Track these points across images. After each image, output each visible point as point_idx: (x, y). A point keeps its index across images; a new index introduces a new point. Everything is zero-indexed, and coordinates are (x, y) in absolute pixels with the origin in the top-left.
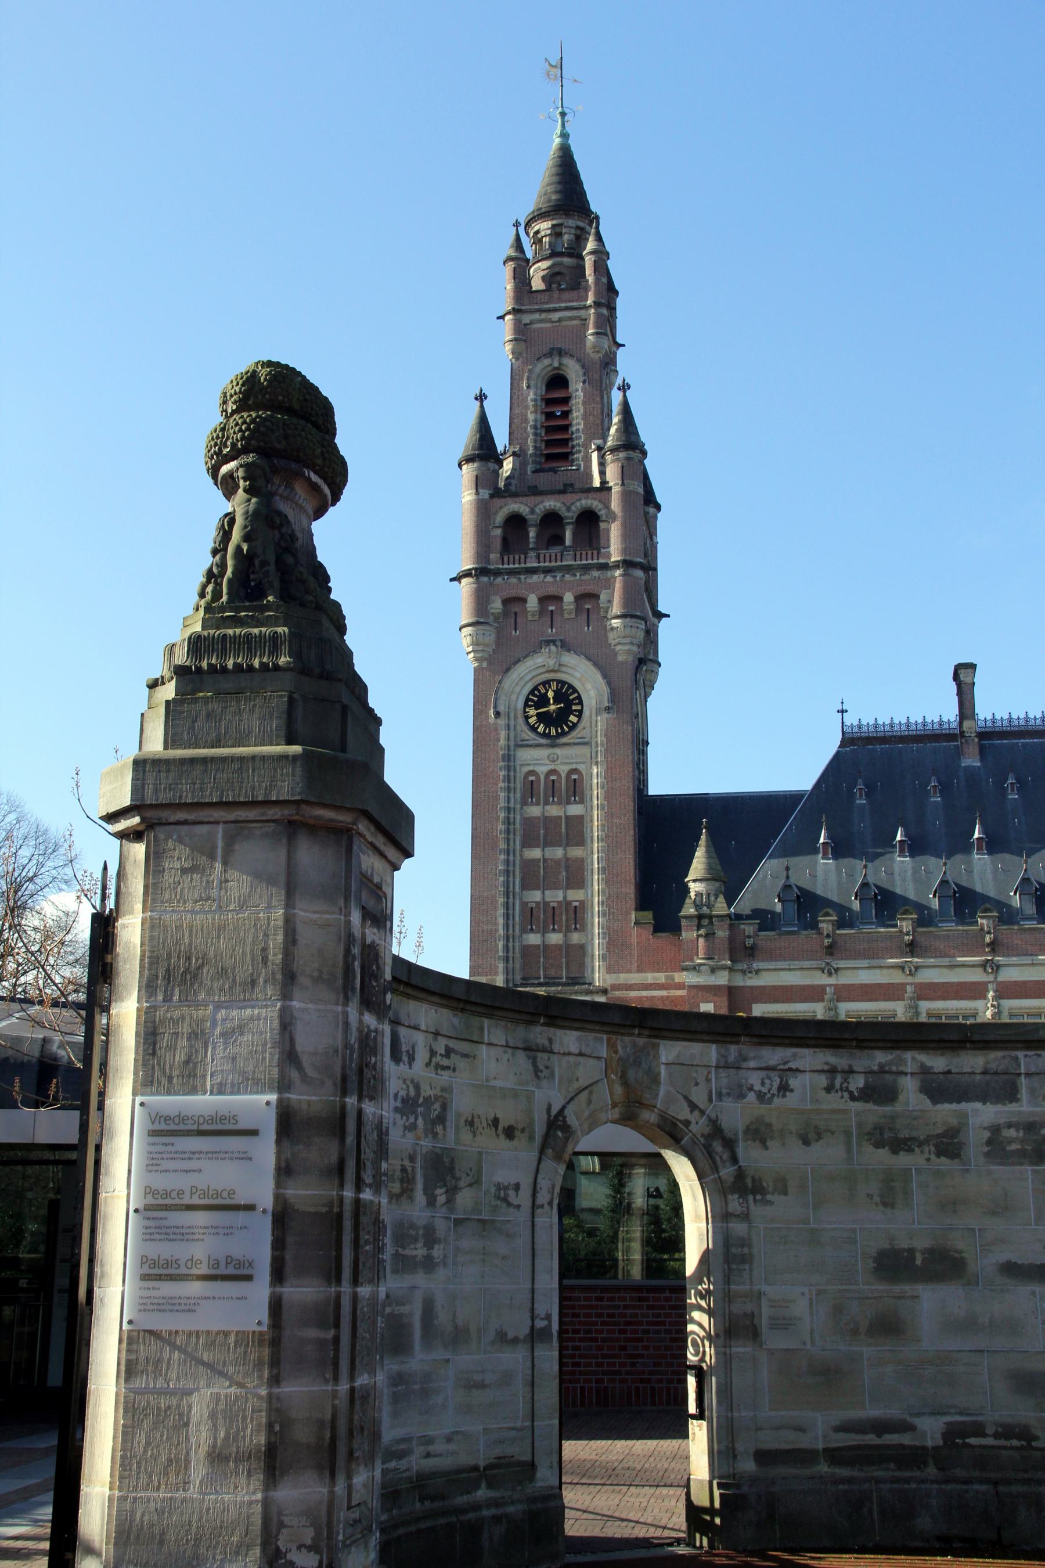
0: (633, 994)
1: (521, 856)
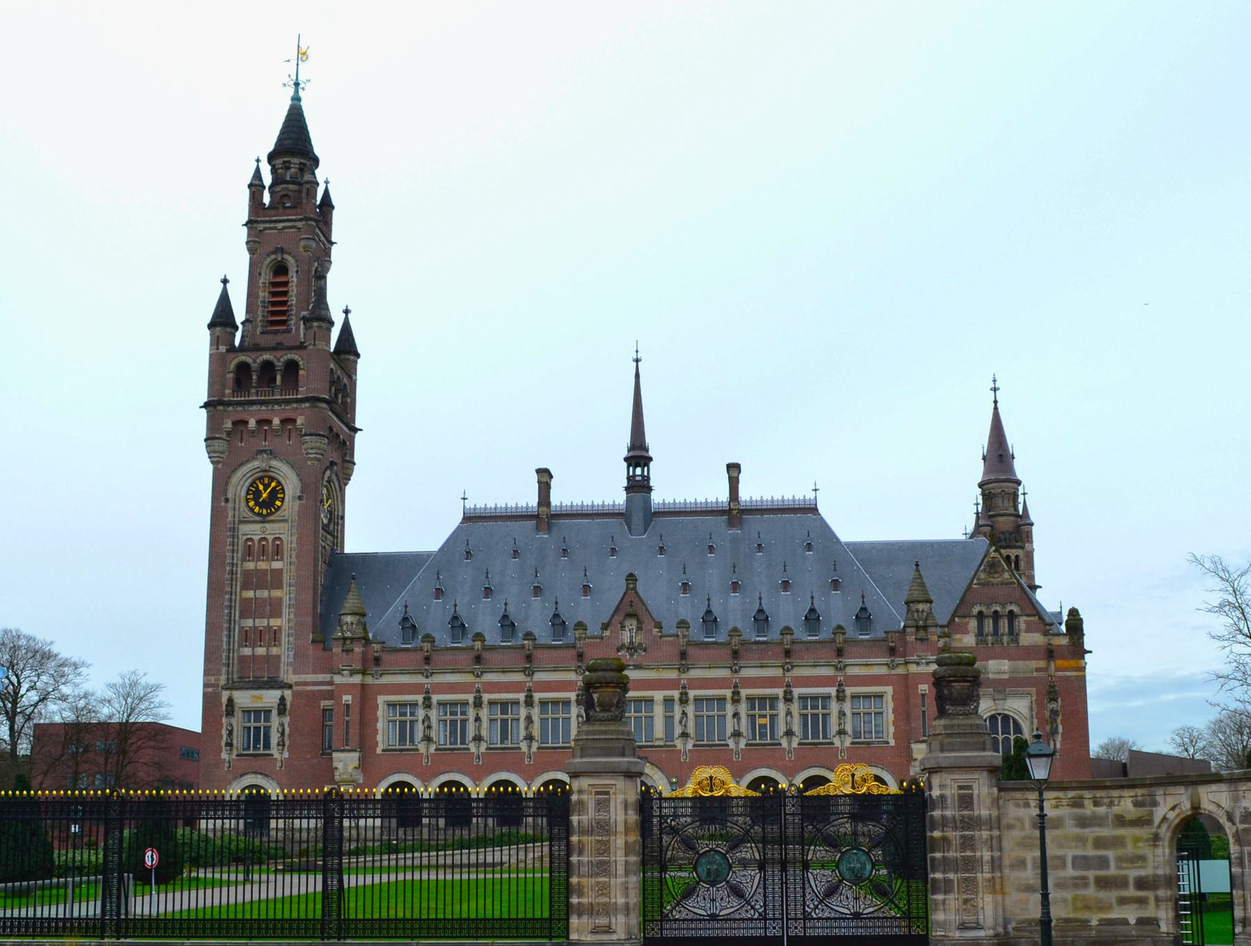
0: (309, 688)
1: (241, 596)
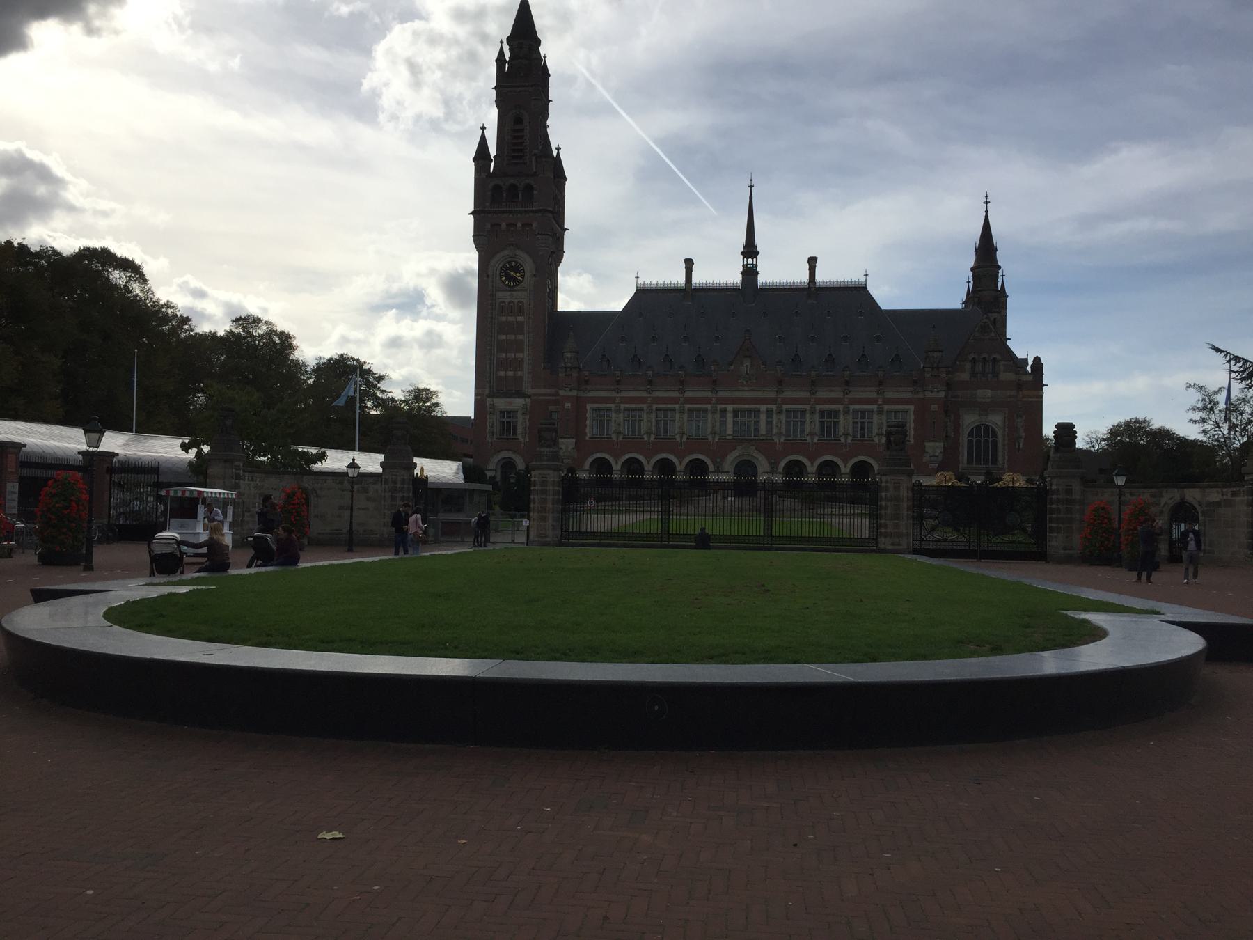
0: (541, 398)
